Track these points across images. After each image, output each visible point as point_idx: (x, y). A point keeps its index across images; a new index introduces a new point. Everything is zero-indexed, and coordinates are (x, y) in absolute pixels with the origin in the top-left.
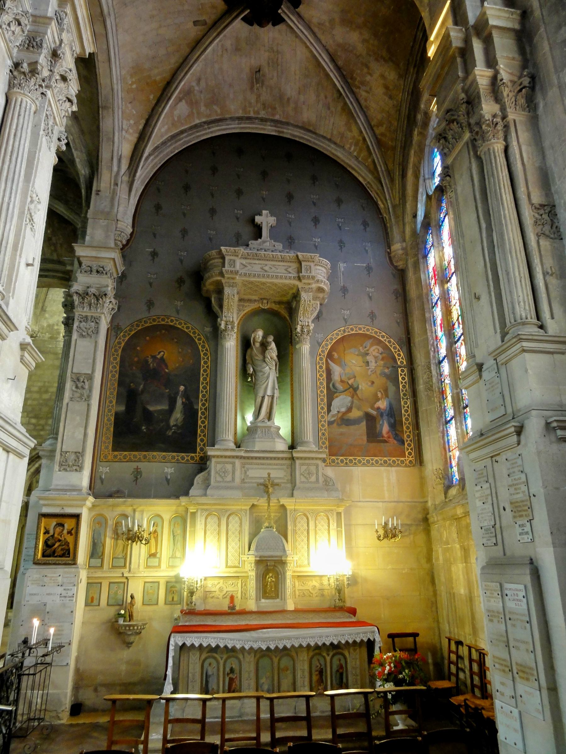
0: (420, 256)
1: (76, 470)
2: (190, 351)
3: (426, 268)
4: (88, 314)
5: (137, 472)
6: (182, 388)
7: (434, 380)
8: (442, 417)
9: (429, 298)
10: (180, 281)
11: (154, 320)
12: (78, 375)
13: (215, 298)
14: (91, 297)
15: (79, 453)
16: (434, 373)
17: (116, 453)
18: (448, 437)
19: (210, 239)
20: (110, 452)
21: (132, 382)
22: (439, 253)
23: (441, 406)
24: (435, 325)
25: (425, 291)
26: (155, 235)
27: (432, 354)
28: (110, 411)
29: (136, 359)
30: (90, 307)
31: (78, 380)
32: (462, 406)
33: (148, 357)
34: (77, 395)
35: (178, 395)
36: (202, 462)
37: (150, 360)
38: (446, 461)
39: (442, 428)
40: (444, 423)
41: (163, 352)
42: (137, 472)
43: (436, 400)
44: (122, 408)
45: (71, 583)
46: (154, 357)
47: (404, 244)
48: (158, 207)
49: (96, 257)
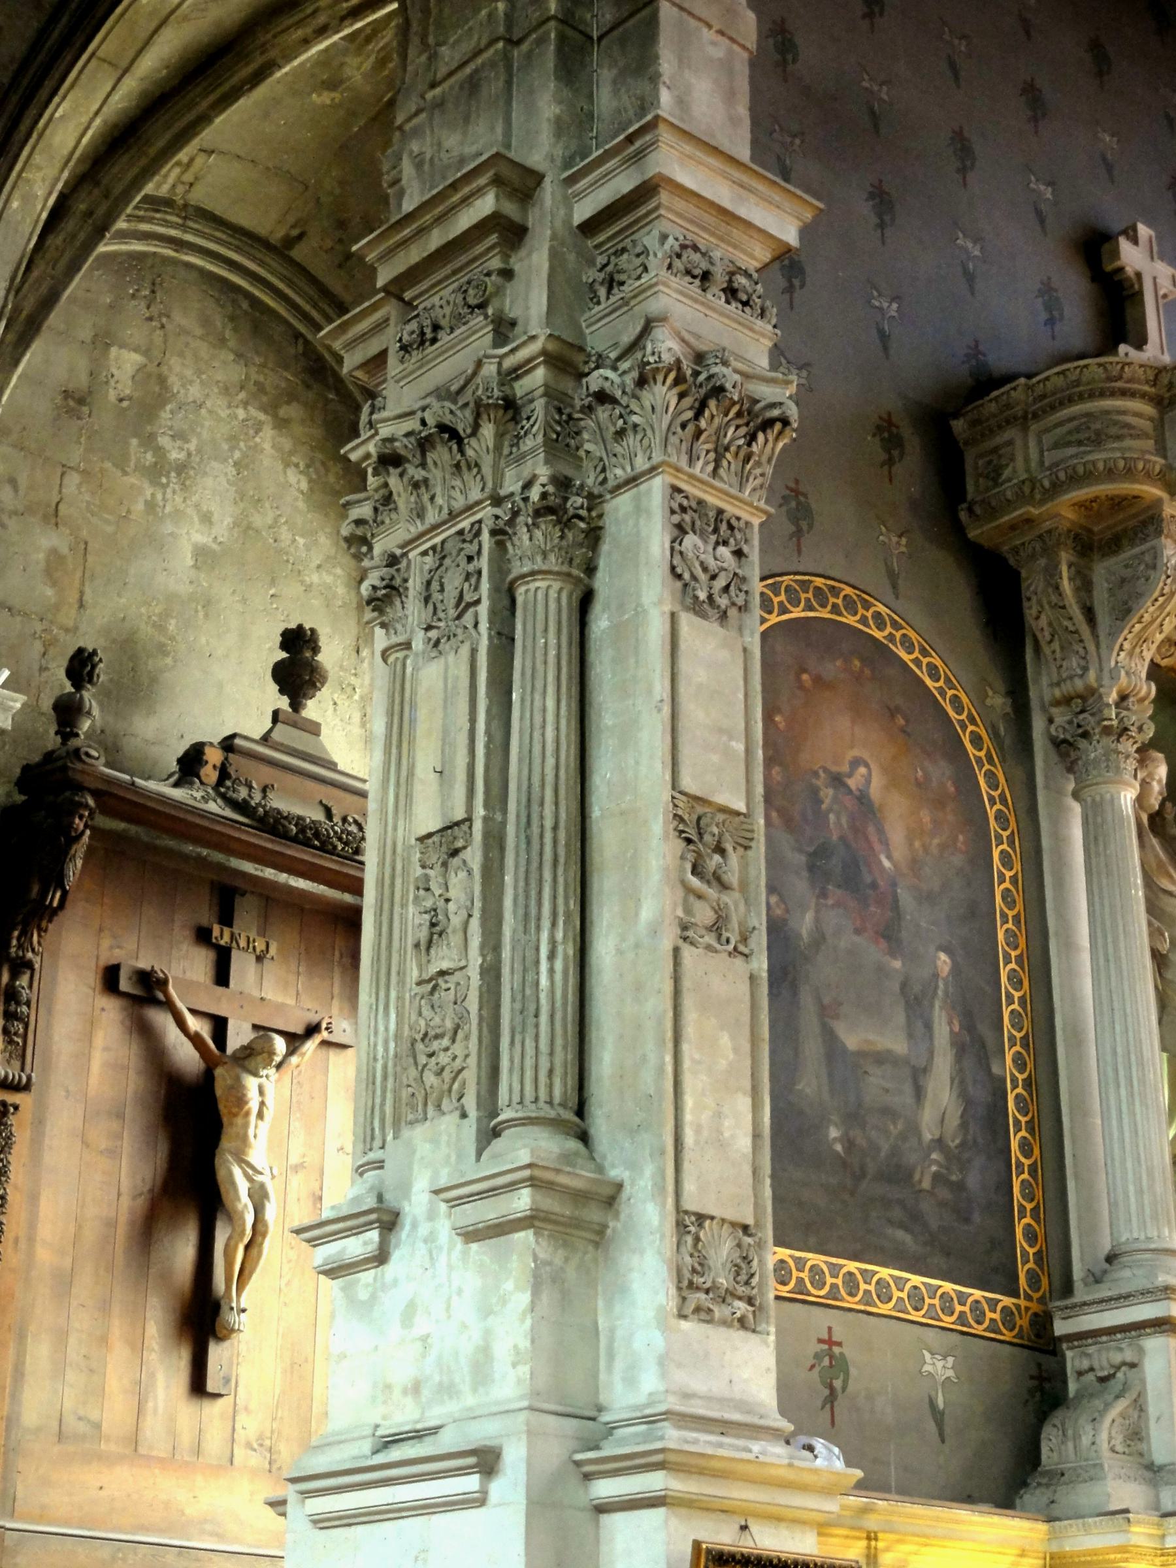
1: (742, 1323)
5: (832, 1357)
15: (745, 1228)
19: (970, 278)
34: (704, 914)
37: (828, 794)
41: (867, 765)
49: (723, 212)
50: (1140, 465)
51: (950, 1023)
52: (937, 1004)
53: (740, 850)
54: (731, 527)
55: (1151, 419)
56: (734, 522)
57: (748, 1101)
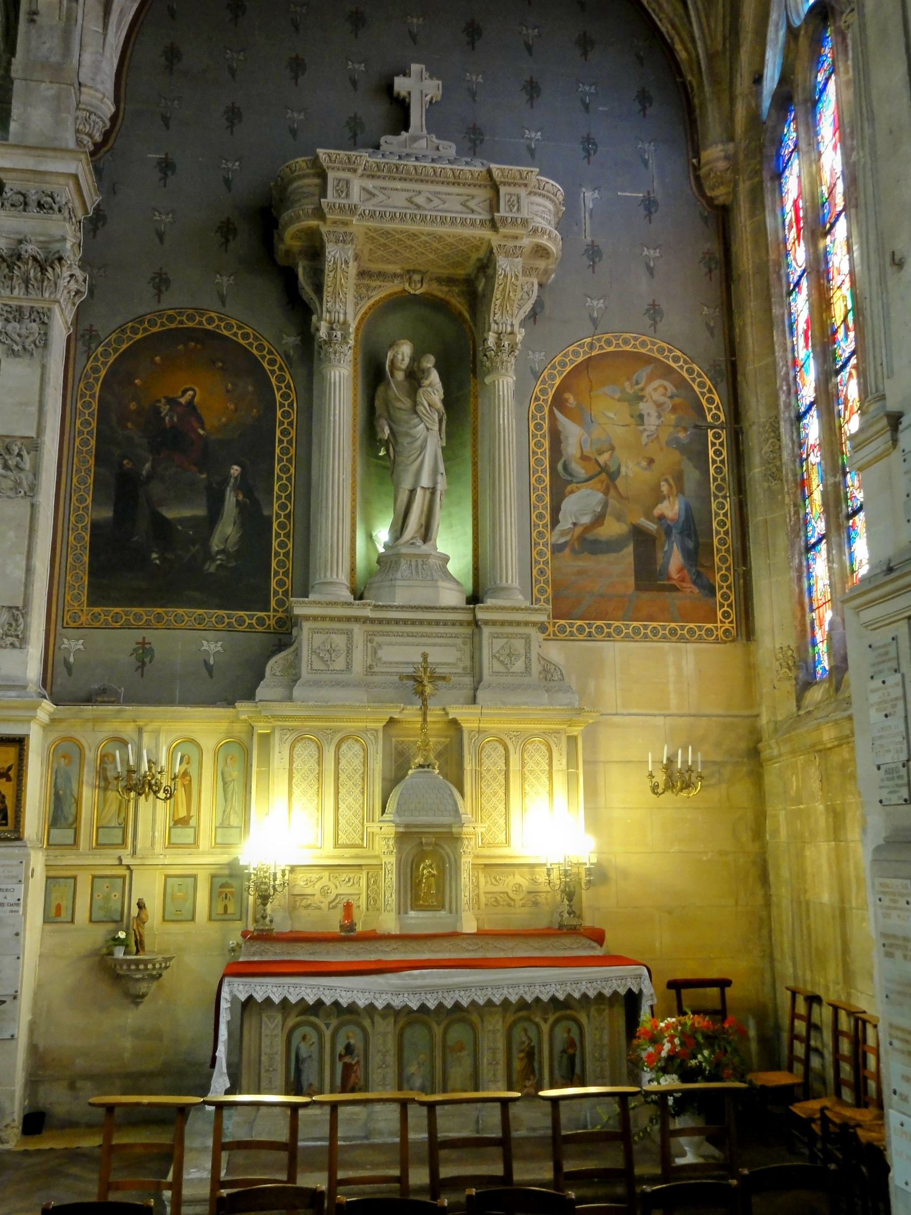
0: (766, 175)
1: (13, 645)
2: (250, 388)
3: (778, 203)
4: (24, 304)
6: (235, 470)
7: (786, 456)
8: (798, 536)
9: (782, 272)
10: (227, 230)
11: (171, 319)
12: (7, 440)
13: (304, 268)
14: (28, 264)
15: (17, 608)
16: (785, 439)
17: (97, 610)
18: (809, 579)
19: (294, 132)
20: (85, 608)
21: (125, 457)
22: (810, 165)
23: (797, 513)
24: (792, 334)
25: (773, 256)
26: (166, 121)
27: (783, 397)
28: (79, 519)
29: (133, 406)
30: (27, 288)
31: (8, 450)
32: (844, 512)
33: (159, 401)
35: (228, 483)
36: (281, 630)
37: (165, 409)
38: (803, 631)
39: (797, 561)
40: (803, 550)
42: (144, 649)
43: (787, 500)
44: (107, 513)
45: (12, 877)
46: (172, 402)
47: (731, 146)
48: (172, 55)
50: (301, 213)
51: (236, 497)
52: (228, 489)
53: (33, 453)
54: (38, 313)
55: (316, 185)
56: (40, 310)
57: (24, 557)
